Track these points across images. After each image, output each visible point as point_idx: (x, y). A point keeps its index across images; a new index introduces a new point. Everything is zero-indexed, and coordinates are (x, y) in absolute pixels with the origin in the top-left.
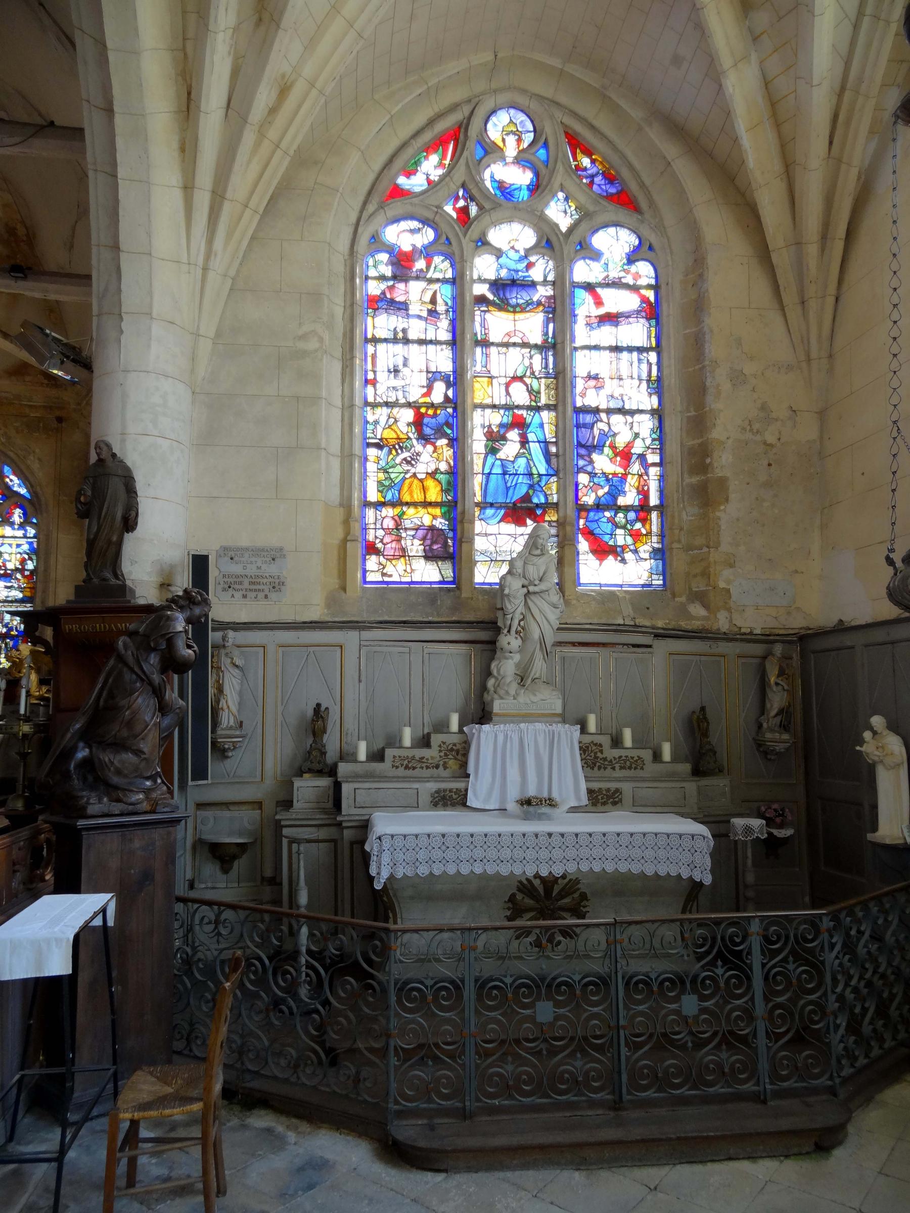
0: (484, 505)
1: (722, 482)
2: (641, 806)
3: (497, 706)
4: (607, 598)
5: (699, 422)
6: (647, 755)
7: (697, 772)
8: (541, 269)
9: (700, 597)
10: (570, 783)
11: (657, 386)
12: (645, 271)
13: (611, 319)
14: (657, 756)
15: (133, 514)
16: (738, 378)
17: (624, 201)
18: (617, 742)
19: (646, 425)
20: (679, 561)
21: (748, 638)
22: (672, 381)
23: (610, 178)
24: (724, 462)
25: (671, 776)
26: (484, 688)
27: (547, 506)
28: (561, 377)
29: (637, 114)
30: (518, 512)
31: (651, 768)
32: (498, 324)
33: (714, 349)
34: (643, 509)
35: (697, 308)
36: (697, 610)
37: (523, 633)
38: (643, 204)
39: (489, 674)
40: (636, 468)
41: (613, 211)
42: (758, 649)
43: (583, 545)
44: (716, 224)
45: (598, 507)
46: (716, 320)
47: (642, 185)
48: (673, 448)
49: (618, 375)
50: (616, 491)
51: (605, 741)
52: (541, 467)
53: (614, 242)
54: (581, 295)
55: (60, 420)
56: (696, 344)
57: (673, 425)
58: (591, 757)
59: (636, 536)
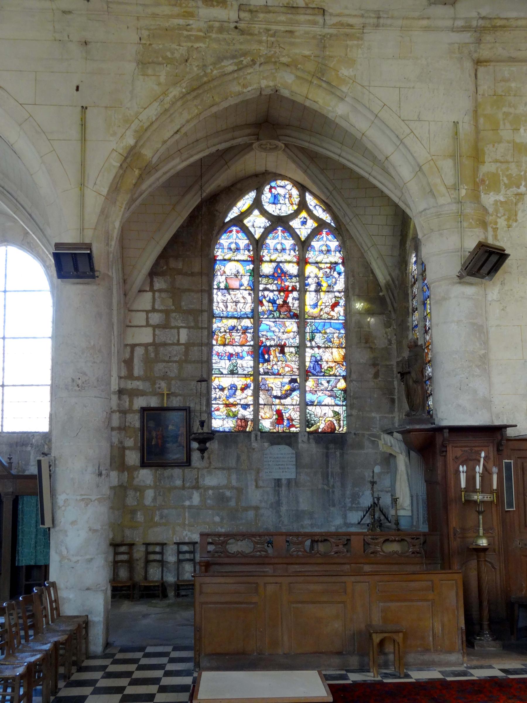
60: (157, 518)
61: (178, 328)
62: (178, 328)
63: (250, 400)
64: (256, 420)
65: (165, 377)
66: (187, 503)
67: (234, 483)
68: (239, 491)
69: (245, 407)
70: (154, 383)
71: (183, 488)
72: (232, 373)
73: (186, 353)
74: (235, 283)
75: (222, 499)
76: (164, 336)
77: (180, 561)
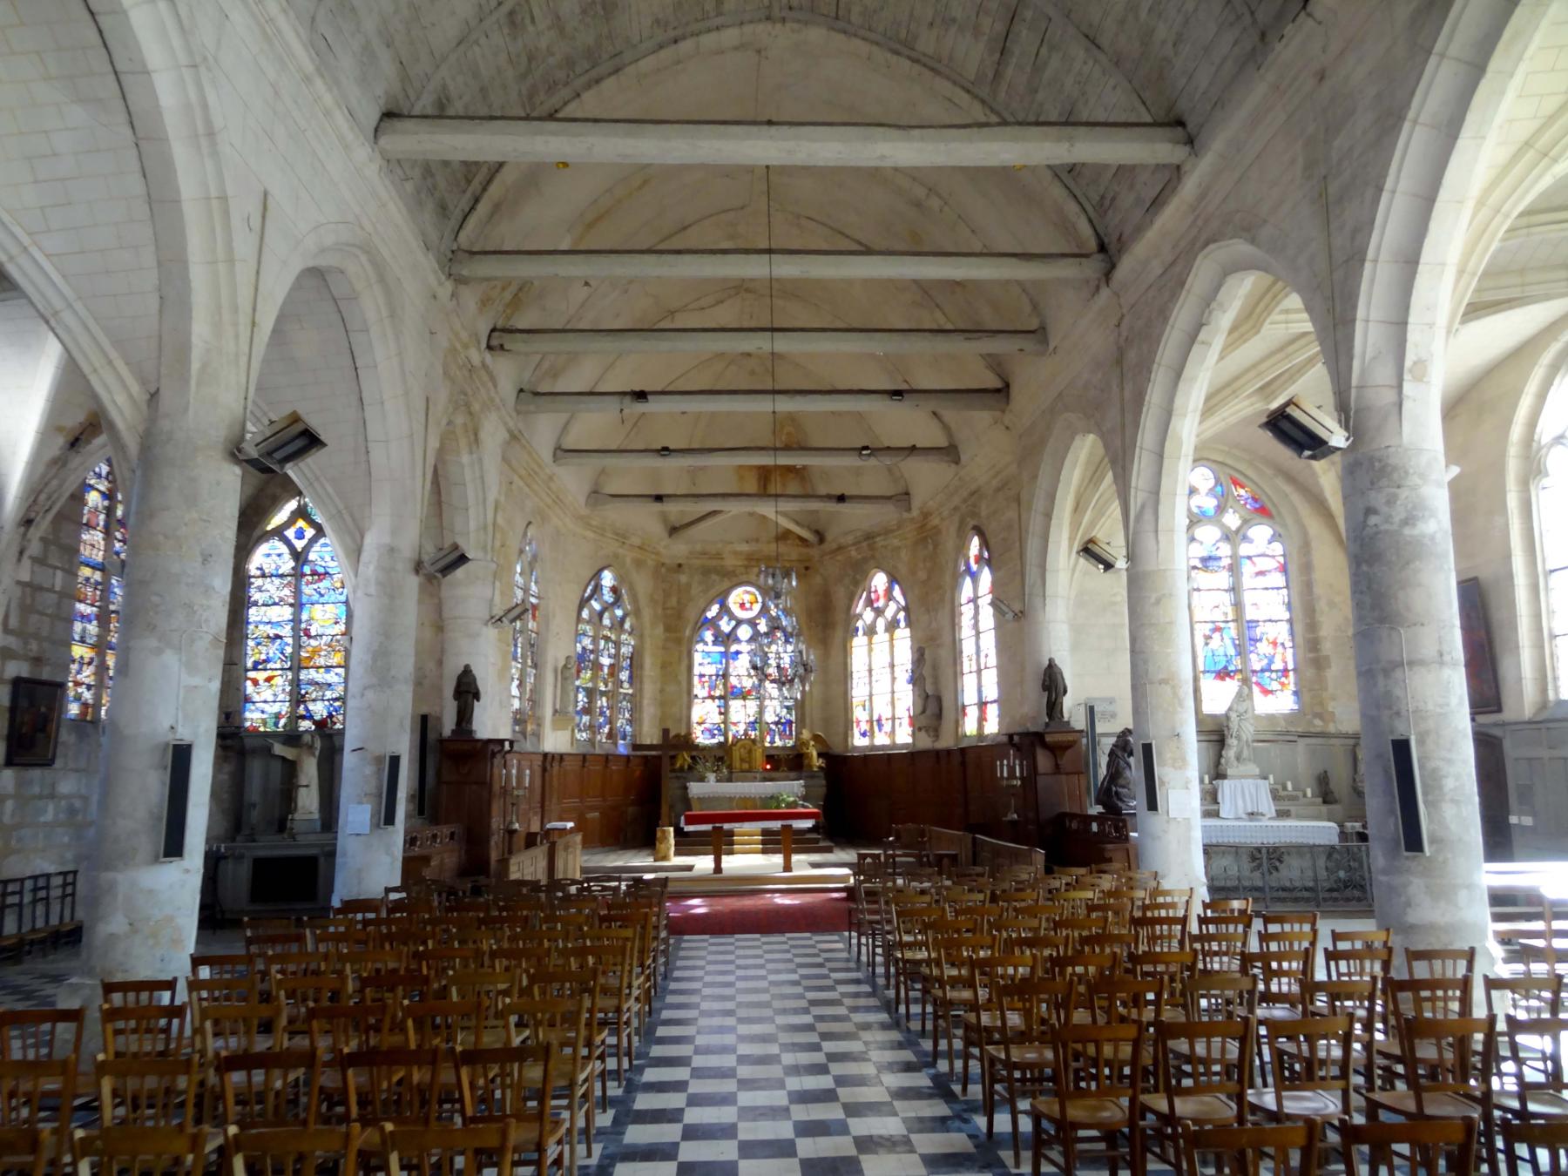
0: (1204, 672)
1: (1327, 658)
2: (1300, 817)
3: (1229, 772)
4: (1271, 718)
5: (1312, 626)
6: (1300, 794)
7: (1325, 802)
8: (1225, 550)
9: (1319, 716)
10: (1268, 806)
11: (1289, 606)
12: (1278, 548)
13: (1261, 573)
14: (1305, 795)
15: (944, 653)
16: (1331, 604)
17: (1263, 511)
18: (1285, 788)
19: (1285, 627)
20: (1307, 697)
21: (1346, 736)
22: (1296, 603)
23: (1255, 500)
24: (1327, 647)
25: (1313, 804)
26: (1218, 763)
27: (1236, 672)
28: (1238, 606)
29: (1269, 472)
30: (1223, 674)
31: (1302, 800)
32: (1202, 579)
33: (1319, 590)
34: (1285, 672)
35: (1307, 568)
36: (1318, 722)
37: (1238, 738)
38: (1274, 512)
39: (1220, 756)
40: (1280, 649)
41: (1259, 518)
42: (1352, 742)
43: (1256, 689)
44: (1315, 527)
45: (1263, 671)
46: (1318, 575)
47: (1274, 505)
48: (1299, 640)
49: (1269, 604)
50: (1271, 660)
51: (1279, 787)
52: (1232, 651)
53: (1261, 533)
54: (1246, 563)
55: (807, 568)
56: (1308, 586)
57: (1299, 628)
58: (1276, 796)
59: (1283, 684)
60: (13, 842)
61: (56, 568)
62: (56, 568)
63: (91, 681)
64: (97, 706)
65: (36, 636)
66: (42, 819)
67: (83, 791)
68: (85, 799)
69: (89, 687)
70: (26, 643)
71: (40, 797)
72: (83, 641)
73: (59, 605)
74: (93, 523)
75: (72, 811)
76: (43, 577)
77: (34, 902)
